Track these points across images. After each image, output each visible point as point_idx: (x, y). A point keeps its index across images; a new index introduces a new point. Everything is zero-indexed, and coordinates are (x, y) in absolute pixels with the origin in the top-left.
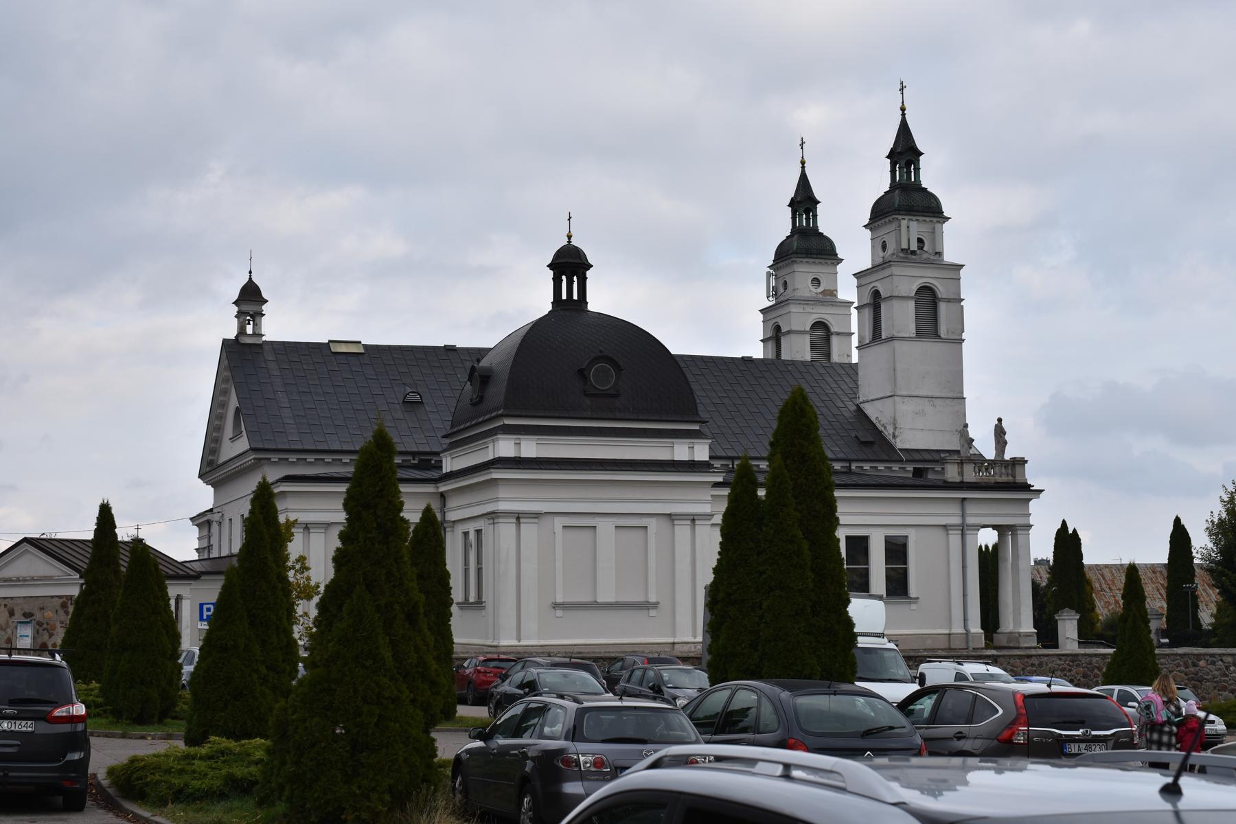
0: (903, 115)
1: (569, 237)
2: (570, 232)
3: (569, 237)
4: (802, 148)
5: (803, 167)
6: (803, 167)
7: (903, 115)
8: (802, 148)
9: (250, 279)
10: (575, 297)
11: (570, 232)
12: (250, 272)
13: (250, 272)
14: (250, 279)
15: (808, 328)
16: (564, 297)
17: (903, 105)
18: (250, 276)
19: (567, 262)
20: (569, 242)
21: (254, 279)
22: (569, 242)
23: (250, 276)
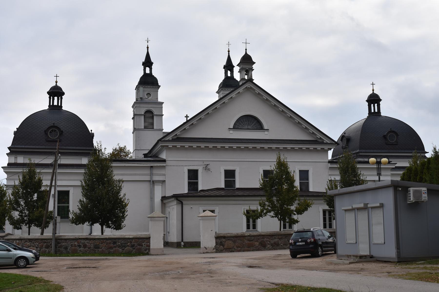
0: (229, 53)
1: (373, 90)
2: (373, 89)
3: (373, 90)
4: (148, 42)
5: (148, 50)
6: (148, 50)
7: (229, 53)
8: (148, 42)
9: (246, 53)
10: (376, 111)
11: (373, 89)
12: (246, 50)
13: (246, 50)
14: (246, 53)
15: (143, 113)
16: (373, 111)
17: (229, 50)
18: (246, 51)
19: (374, 99)
20: (373, 92)
21: (248, 53)
22: (373, 92)
23: (246, 51)
